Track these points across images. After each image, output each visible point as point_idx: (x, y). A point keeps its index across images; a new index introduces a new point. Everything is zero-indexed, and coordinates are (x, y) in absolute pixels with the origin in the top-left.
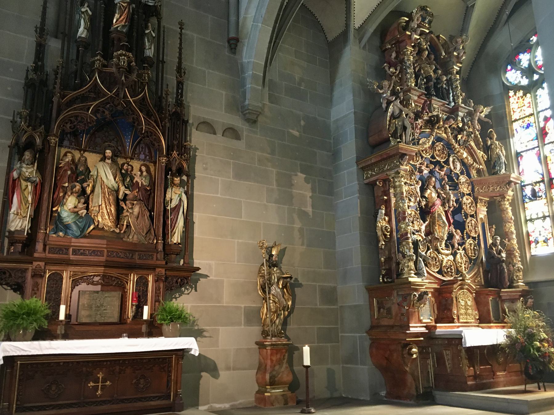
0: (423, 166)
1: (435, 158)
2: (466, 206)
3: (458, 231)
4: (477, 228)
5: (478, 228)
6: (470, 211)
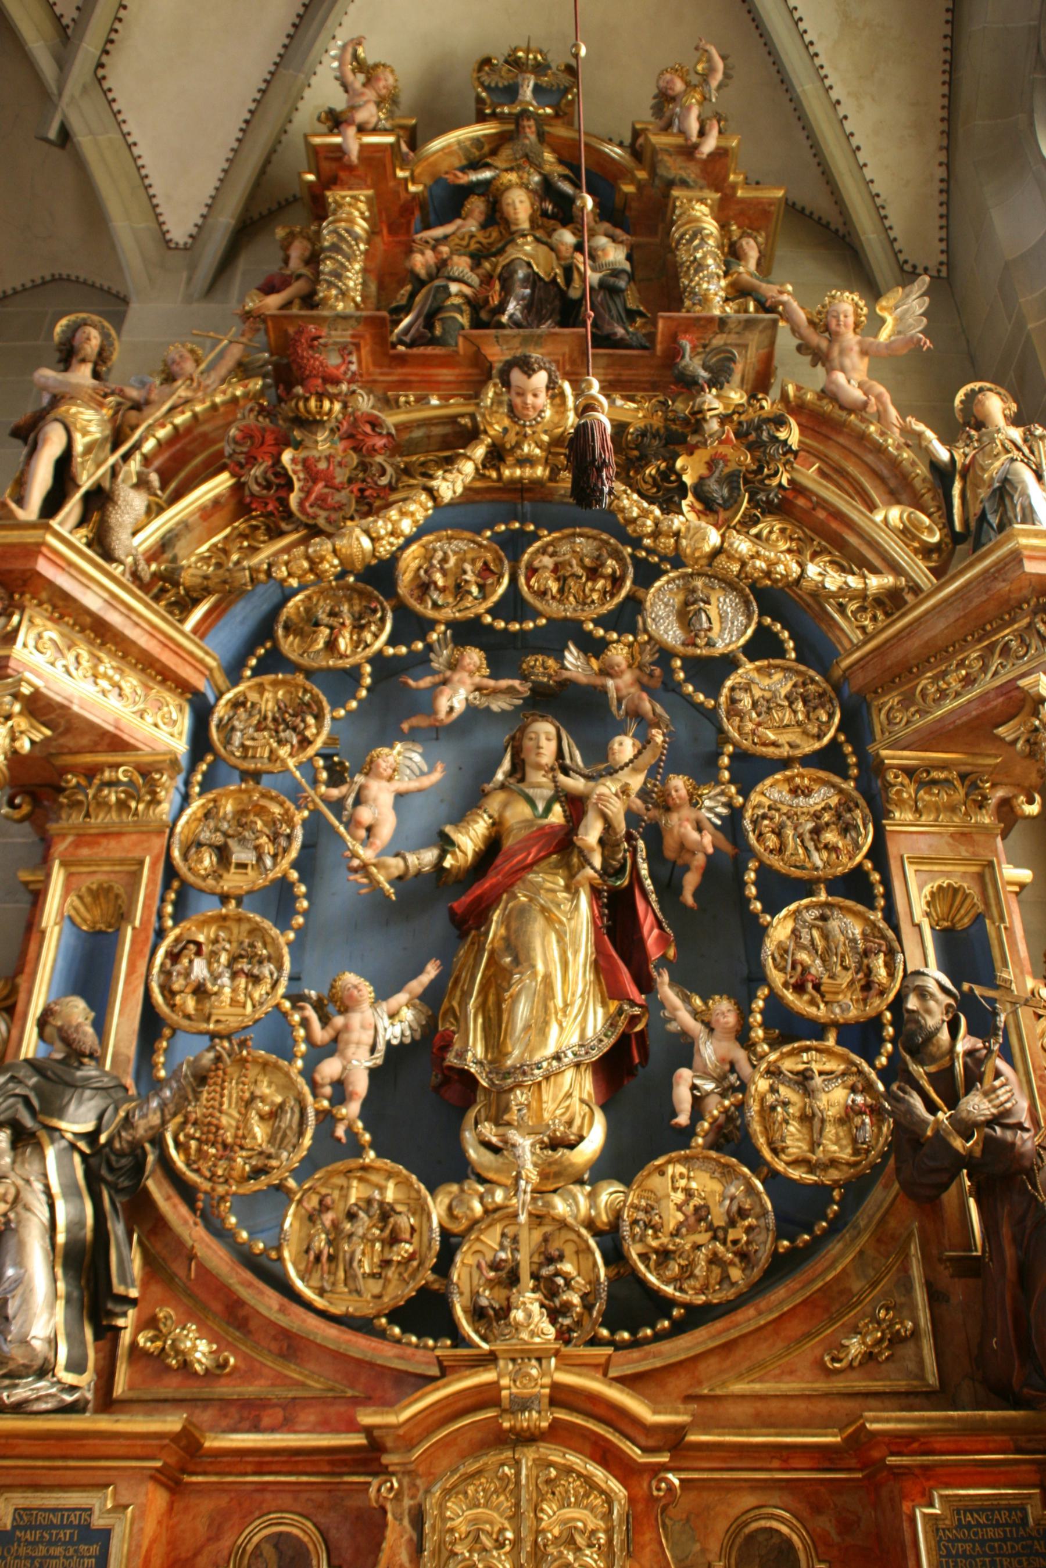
1: (536, 614)
2: (779, 833)
3: (724, 1010)
4: (879, 963)
5: (891, 953)
6: (818, 859)
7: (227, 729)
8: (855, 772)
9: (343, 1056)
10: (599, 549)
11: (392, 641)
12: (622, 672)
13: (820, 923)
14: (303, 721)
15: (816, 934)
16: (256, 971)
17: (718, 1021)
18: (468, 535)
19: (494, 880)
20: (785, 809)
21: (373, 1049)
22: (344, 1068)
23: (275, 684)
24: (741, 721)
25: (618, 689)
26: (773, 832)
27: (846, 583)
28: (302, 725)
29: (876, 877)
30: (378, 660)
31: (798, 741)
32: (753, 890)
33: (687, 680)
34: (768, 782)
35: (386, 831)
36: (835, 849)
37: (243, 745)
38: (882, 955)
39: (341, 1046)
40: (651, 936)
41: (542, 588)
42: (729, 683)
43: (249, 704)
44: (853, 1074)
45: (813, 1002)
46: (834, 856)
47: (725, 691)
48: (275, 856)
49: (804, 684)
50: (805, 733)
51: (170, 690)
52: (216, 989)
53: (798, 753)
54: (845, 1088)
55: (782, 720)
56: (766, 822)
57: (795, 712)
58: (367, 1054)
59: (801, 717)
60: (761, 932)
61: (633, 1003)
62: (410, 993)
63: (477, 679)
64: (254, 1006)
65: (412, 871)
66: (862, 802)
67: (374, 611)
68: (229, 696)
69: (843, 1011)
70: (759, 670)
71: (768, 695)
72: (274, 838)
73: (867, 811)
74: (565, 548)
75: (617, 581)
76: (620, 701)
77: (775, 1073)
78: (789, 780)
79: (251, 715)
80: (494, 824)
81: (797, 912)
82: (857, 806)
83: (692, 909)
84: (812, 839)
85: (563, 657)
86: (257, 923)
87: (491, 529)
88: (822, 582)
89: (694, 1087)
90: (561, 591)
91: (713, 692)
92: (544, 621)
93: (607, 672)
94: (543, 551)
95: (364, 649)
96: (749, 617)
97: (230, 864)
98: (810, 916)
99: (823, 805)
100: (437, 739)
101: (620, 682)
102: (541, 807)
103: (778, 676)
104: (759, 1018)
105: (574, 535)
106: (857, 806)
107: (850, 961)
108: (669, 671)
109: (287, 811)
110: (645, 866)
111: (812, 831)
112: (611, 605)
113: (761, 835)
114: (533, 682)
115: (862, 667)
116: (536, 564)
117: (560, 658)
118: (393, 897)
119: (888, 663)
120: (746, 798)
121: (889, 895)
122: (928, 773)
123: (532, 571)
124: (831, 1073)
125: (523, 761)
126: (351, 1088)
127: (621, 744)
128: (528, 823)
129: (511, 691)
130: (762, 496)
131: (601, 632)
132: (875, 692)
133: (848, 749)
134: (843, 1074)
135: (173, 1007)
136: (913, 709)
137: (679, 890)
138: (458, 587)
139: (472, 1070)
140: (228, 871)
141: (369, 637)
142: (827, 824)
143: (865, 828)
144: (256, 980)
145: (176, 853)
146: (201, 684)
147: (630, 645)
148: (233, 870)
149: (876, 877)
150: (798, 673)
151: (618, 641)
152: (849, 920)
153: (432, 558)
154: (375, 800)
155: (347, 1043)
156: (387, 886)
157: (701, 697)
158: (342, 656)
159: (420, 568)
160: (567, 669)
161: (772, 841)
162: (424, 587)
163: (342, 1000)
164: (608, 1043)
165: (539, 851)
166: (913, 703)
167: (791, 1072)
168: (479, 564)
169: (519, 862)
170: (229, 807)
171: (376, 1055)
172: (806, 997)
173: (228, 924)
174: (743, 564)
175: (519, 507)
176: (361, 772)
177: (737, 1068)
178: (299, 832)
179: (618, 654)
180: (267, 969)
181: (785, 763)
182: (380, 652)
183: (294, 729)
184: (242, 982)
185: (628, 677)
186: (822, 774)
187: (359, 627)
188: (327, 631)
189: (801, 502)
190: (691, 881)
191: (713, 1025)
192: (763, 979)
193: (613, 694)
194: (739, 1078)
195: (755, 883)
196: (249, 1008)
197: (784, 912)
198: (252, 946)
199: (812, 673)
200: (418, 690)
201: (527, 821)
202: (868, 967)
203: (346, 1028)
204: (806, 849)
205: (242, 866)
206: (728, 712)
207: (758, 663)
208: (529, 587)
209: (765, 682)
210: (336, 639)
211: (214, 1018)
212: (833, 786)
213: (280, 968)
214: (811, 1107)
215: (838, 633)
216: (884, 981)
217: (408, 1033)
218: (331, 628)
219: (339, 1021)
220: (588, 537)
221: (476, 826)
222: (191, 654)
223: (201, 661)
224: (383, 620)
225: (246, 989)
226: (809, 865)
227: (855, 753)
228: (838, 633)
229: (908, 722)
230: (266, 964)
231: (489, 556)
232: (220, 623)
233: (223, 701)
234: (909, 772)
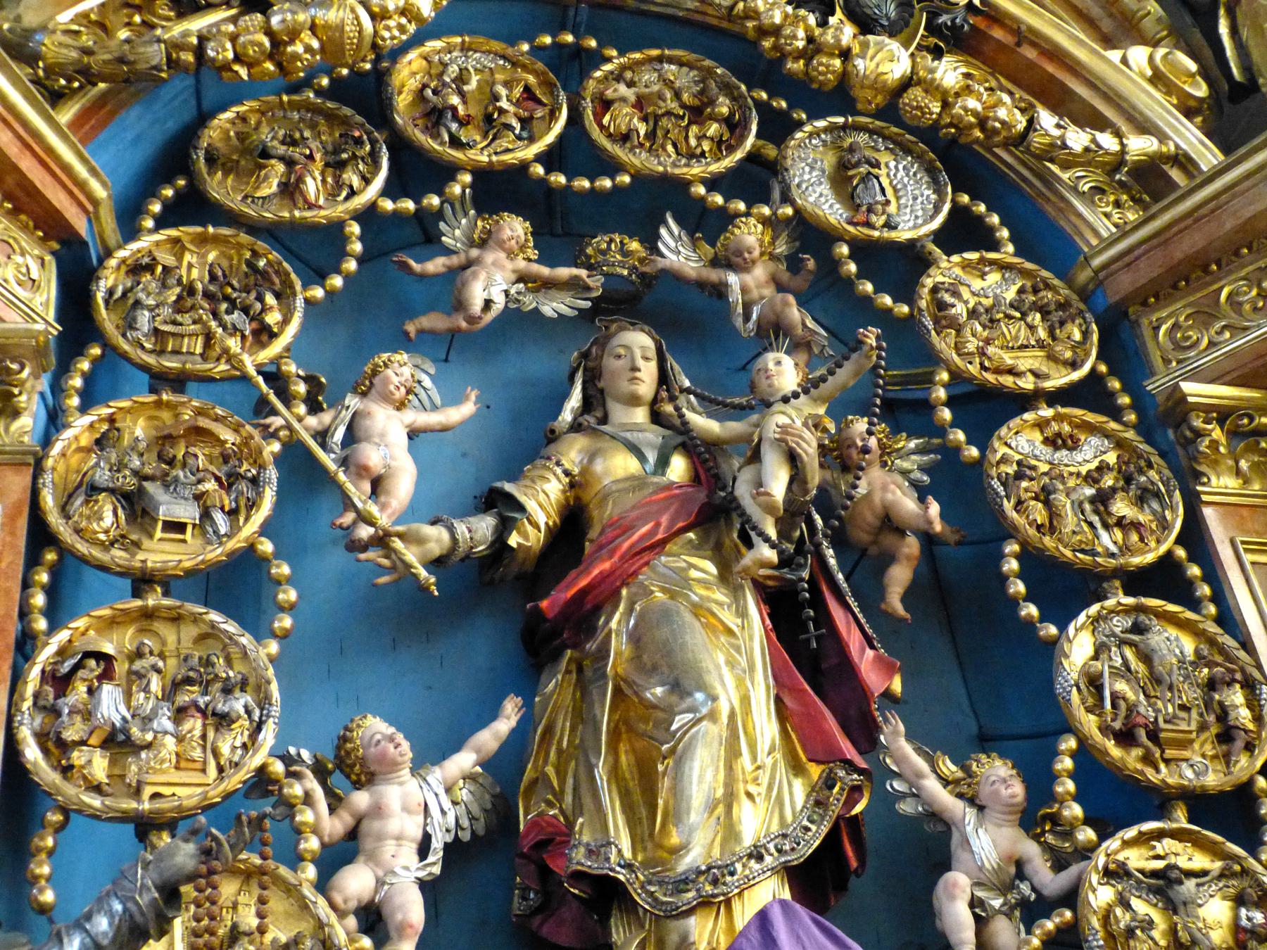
0: (491, 256)
1: (612, 167)
2: (1045, 496)
4: (1236, 697)
6: (1107, 540)
7: (127, 305)
8: (1132, 417)
9: (373, 858)
10: (703, 81)
11: (387, 192)
12: (754, 262)
13: (1136, 638)
14: (260, 298)
15: (1129, 653)
16: (221, 707)
17: (997, 793)
18: (497, 46)
19: (606, 565)
20: (1044, 468)
21: (424, 850)
22: (380, 883)
23: (202, 240)
24: (958, 331)
25: (744, 290)
26: (1036, 498)
27: (1094, 141)
28: (258, 306)
29: (1195, 571)
30: (368, 216)
31: (1045, 369)
32: (1019, 587)
33: (861, 275)
34: (1015, 422)
35: (403, 486)
36: (1137, 526)
37: (156, 331)
38: (1238, 686)
39: (367, 844)
40: (866, 660)
41: (624, 129)
42: (929, 282)
43: (159, 269)
44: (1234, 875)
45: (1148, 759)
46: (1135, 537)
47: (925, 292)
48: (233, 513)
49: (1036, 291)
50: (1052, 357)
51: (24, 228)
52: (149, 737)
53: (1049, 385)
54: (1224, 898)
55: (1016, 338)
56: (1024, 484)
57: (1032, 328)
58: (416, 858)
59: (1042, 334)
60: (1050, 651)
61: (850, 765)
62: (478, 751)
63: (521, 264)
64: (221, 770)
65: (462, 548)
66: (1155, 459)
67: (359, 142)
68: (121, 254)
69: (1197, 774)
70: (966, 266)
71: (988, 302)
72: (229, 482)
73: (1167, 472)
74: (648, 76)
75: (735, 127)
76: (747, 308)
77: (1115, 873)
78: (1041, 425)
79: (164, 286)
80: (572, 485)
81: (1096, 620)
82: (1150, 466)
83: (903, 620)
84: (1096, 512)
85: (658, 237)
86: (213, 625)
87: (530, 40)
88: (1062, 138)
89: (974, 903)
90: (651, 135)
91: (906, 293)
92: (626, 179)
93: (732, 260)
94: (618, 77)
95: (347, 198)
96: (939, 191)
97: (156, 520)
98: (1119, 624)
99: (1095, 464)
100: (446, 360)
101: (749, 279)
102: (652, 457)
103: (994, 277)
104: (1070, 786)
105: (660, 59)
106: (1150, 466)
107: (1190, 694)
108: (830, 265)
109: (247, 440)
110: (831, 552)
111: (1092, 501)
112: (729, 162)
113: (1019, 502)
114: (606, 275)
115: (1128, 265)
116: (609, 93)
117: (651, 241)
118: (436, 593)
119: (1179, 255)
120: (984, 447)
121: (1221, 596)
122: (1252, 419)
123: (605, 105)
124: (1204, 873)
125: (602, 391)
126: (399, 917)
127: (779, 363)
128: (635, 483)
129: (574, 285)
130: (945, 18)
131: (719, 199)
132: (1145, 303)
133: (1116, 384)
134: (1221, 876)
135: (66, 771)
136: (1218, 325)
137: (881, 592)
138: (488, 119)
139: (621, 877)
140: (151, 536)
141: (356, 182)
142: (1114, 490)
143: (1170, 497)
144: (223, 721)
145: (48, 500)
146: (81, 225)
147: (765, 221)
148: (159, 534)
149: (1195, 571)
150: (1024, 273)
151: (748, 214)
152: (1173, 632)
153: (441, 74)
154: (382, 435)
155: (381, 837)
156: (423, 573)
157: (887, 300)
158: (311, 206)
159: (425, 86)
160: (662, 256)
161: (1039, 513)
162: (434, 116)
163: (363, 761)
164: (817, 835)
165: (672, 522)
166: (1214, 317)
167: (1141, 871)
168: (518, 92)
169: (642, 538)
170: (139, 429)
171: (431, 859)
172: (1137, 752)
173: (158, 626)
174: (946, 105)
175: (571, 13)
176: (355, 391)
177: (1028, 869)
178: (272, 473)
179: (750, 234)
180: (238, 704)
181: (1024, 401)
182: (372, 207)
183: (246, 310)
184: (194, 725)
185: (760, 272)
186: (1091, 417)
187: (337, 166)
188: (281, 168)
189: (998, 33)
190: (899, 577)
191: (983, 799)
192: (1067, 727)
193: (736, 296)
194: (1034, 889)
195: (1021, 576)
196: (212, 771)
197: (1082, 618)
198: (208, 663)
199: (1045, 274)
200: (423, 277)
201: (632, 478)
202: (1221, 704)
203: (377, 811)
204: (1091, 525)
205: (179, 527)
206: (936, 321)
207: (967, 255)
208: (601, 127)
209: (977, 284)
210: (300, 180)
211: (148, 791)
212: (1107, 435)
213: (264, 701)
214: (1186, 928)
215: (1073, 218)
216: (1251, 726)
217: (465, 823)
218: (289, 163)
219: (361, 799)
220: (681, 64)
221: (547, 487)
222: (67, 168)
223: (82, 185)
224: (374, 156)
225: (204, 737)
226: (1100, 549)
227: (1126, 389)
228: (1073, 218)
229: (1212, 344)
230: (237, 693)
231: (531, 79)
232: (103, 136)
233: (113, 262)
234: (1222, 414)
